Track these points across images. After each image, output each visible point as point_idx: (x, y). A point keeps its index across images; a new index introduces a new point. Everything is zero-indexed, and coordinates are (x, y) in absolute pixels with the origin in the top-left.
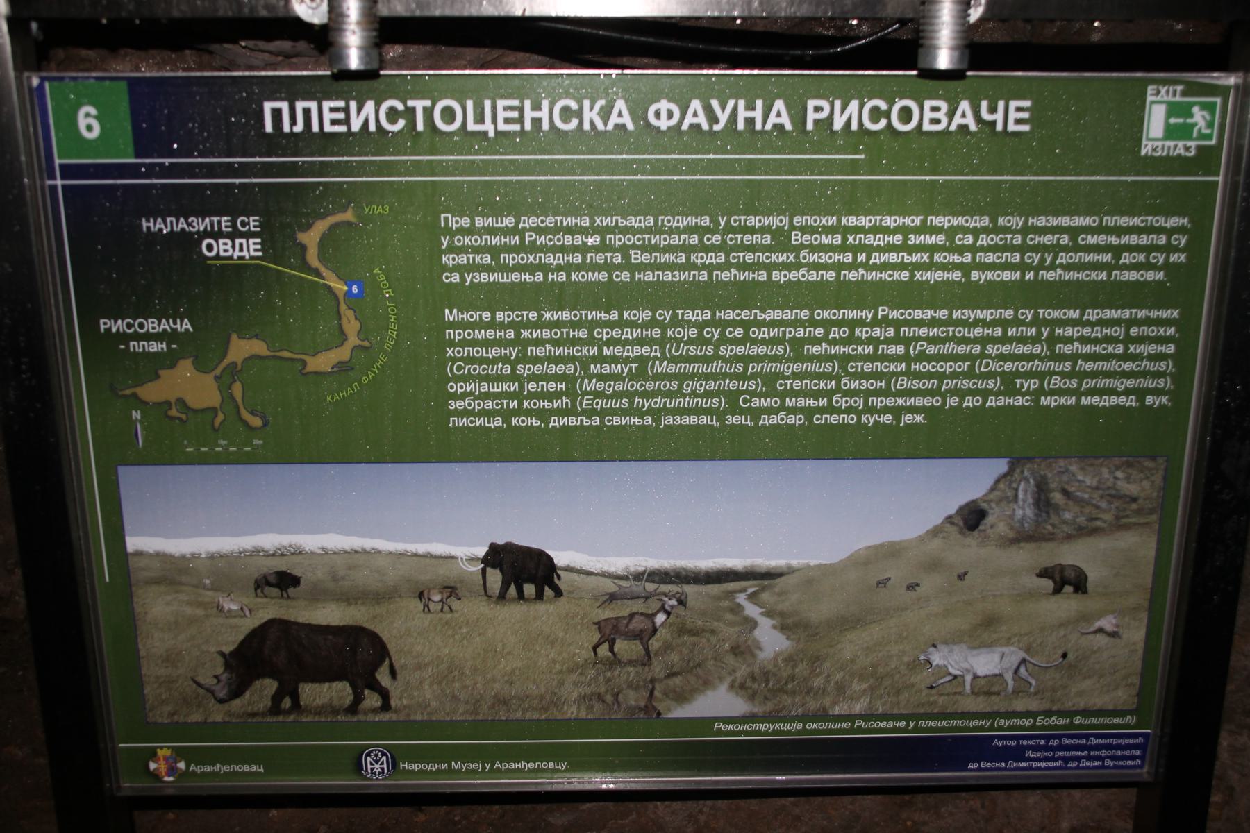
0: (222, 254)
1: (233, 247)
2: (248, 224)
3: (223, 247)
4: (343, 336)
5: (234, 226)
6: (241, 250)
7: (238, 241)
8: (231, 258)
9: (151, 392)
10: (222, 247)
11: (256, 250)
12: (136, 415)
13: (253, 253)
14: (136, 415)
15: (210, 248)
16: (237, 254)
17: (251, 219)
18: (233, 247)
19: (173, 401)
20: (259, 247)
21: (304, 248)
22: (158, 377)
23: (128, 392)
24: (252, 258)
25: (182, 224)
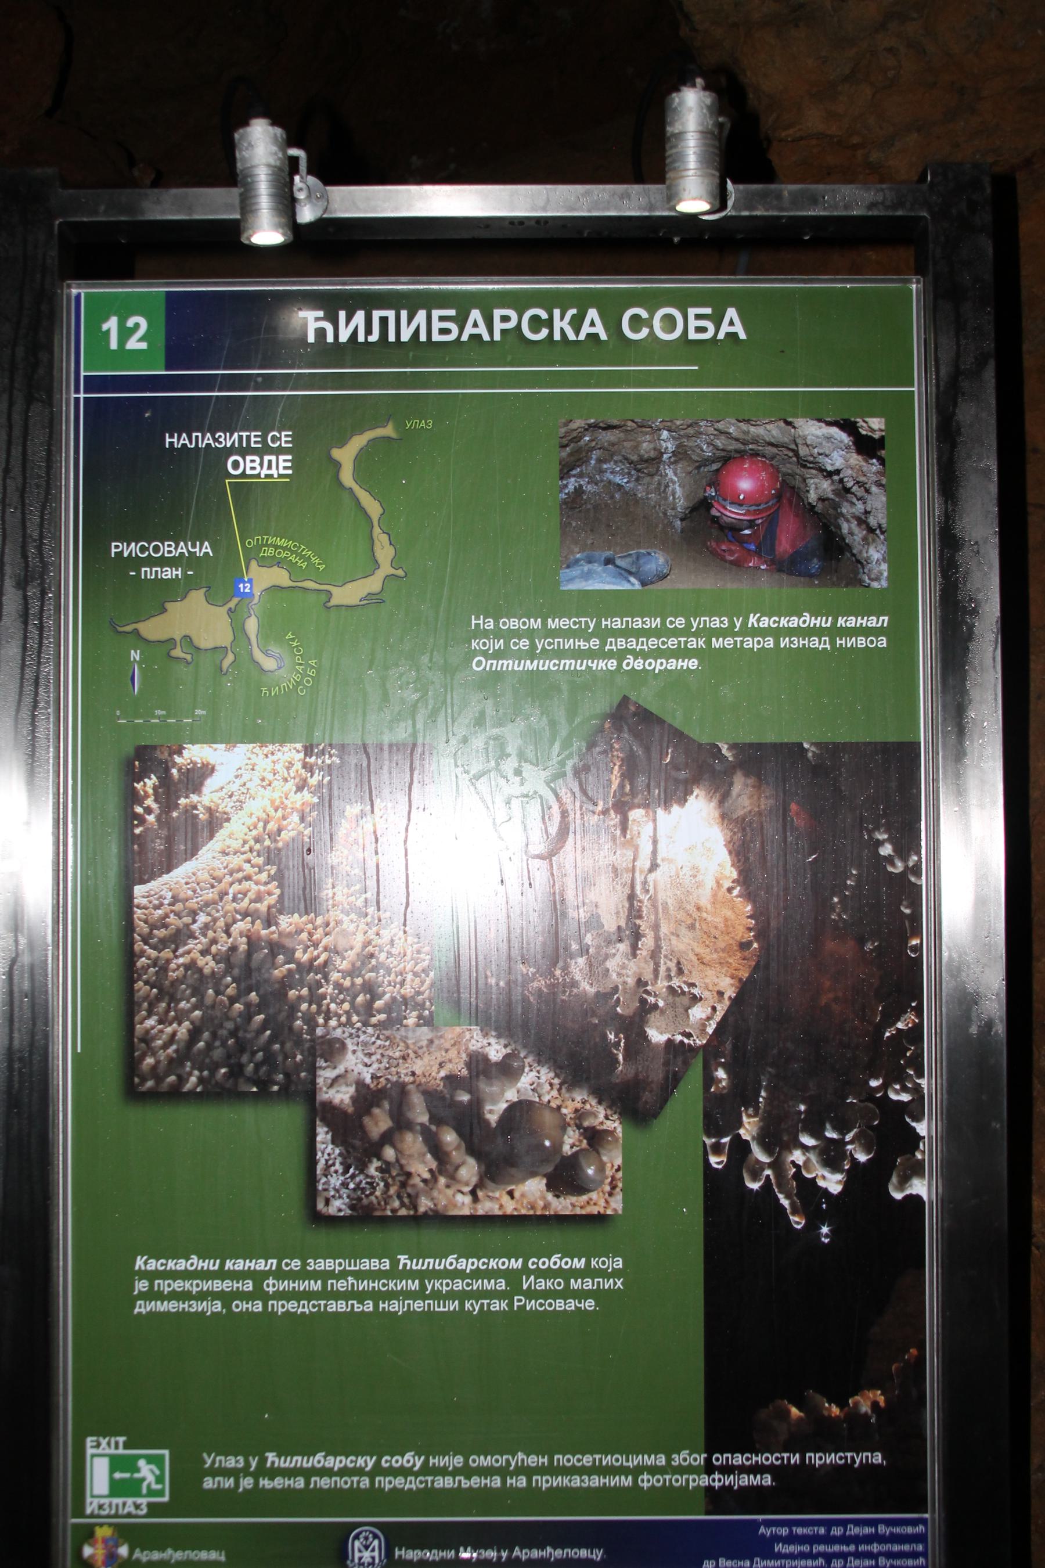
0: (249, 472)
1: (261, 465)
2: (280, 439)
3: (251, 465)
4: (377, 566)
5: (264, 441)
6: (270, 467)
7: (266, 458)
8: (258, 476)
9: (152, 629)
10: (249, 465)
11: (285, 468)
12: (135, 655)
13: (282, 472)
14: (135, 655)
15: (236, 465)
16: (265, 471)
17: (283, 433)
18: (261, 465)
19: (178, 640)
20: (289, 464)
21: (337, 465)
22: (166, 610)
23: (128, 628)
24: (280, 476)
25: (208, 439)
